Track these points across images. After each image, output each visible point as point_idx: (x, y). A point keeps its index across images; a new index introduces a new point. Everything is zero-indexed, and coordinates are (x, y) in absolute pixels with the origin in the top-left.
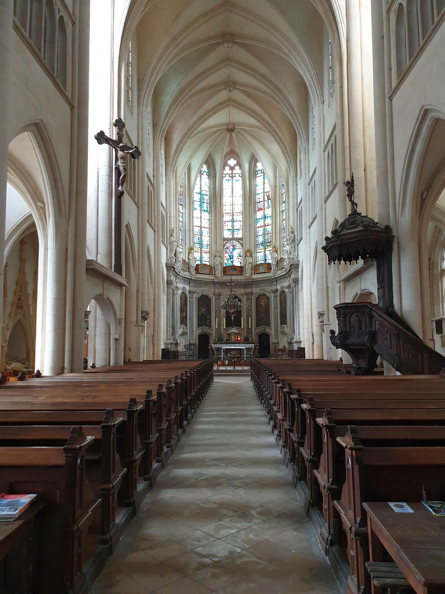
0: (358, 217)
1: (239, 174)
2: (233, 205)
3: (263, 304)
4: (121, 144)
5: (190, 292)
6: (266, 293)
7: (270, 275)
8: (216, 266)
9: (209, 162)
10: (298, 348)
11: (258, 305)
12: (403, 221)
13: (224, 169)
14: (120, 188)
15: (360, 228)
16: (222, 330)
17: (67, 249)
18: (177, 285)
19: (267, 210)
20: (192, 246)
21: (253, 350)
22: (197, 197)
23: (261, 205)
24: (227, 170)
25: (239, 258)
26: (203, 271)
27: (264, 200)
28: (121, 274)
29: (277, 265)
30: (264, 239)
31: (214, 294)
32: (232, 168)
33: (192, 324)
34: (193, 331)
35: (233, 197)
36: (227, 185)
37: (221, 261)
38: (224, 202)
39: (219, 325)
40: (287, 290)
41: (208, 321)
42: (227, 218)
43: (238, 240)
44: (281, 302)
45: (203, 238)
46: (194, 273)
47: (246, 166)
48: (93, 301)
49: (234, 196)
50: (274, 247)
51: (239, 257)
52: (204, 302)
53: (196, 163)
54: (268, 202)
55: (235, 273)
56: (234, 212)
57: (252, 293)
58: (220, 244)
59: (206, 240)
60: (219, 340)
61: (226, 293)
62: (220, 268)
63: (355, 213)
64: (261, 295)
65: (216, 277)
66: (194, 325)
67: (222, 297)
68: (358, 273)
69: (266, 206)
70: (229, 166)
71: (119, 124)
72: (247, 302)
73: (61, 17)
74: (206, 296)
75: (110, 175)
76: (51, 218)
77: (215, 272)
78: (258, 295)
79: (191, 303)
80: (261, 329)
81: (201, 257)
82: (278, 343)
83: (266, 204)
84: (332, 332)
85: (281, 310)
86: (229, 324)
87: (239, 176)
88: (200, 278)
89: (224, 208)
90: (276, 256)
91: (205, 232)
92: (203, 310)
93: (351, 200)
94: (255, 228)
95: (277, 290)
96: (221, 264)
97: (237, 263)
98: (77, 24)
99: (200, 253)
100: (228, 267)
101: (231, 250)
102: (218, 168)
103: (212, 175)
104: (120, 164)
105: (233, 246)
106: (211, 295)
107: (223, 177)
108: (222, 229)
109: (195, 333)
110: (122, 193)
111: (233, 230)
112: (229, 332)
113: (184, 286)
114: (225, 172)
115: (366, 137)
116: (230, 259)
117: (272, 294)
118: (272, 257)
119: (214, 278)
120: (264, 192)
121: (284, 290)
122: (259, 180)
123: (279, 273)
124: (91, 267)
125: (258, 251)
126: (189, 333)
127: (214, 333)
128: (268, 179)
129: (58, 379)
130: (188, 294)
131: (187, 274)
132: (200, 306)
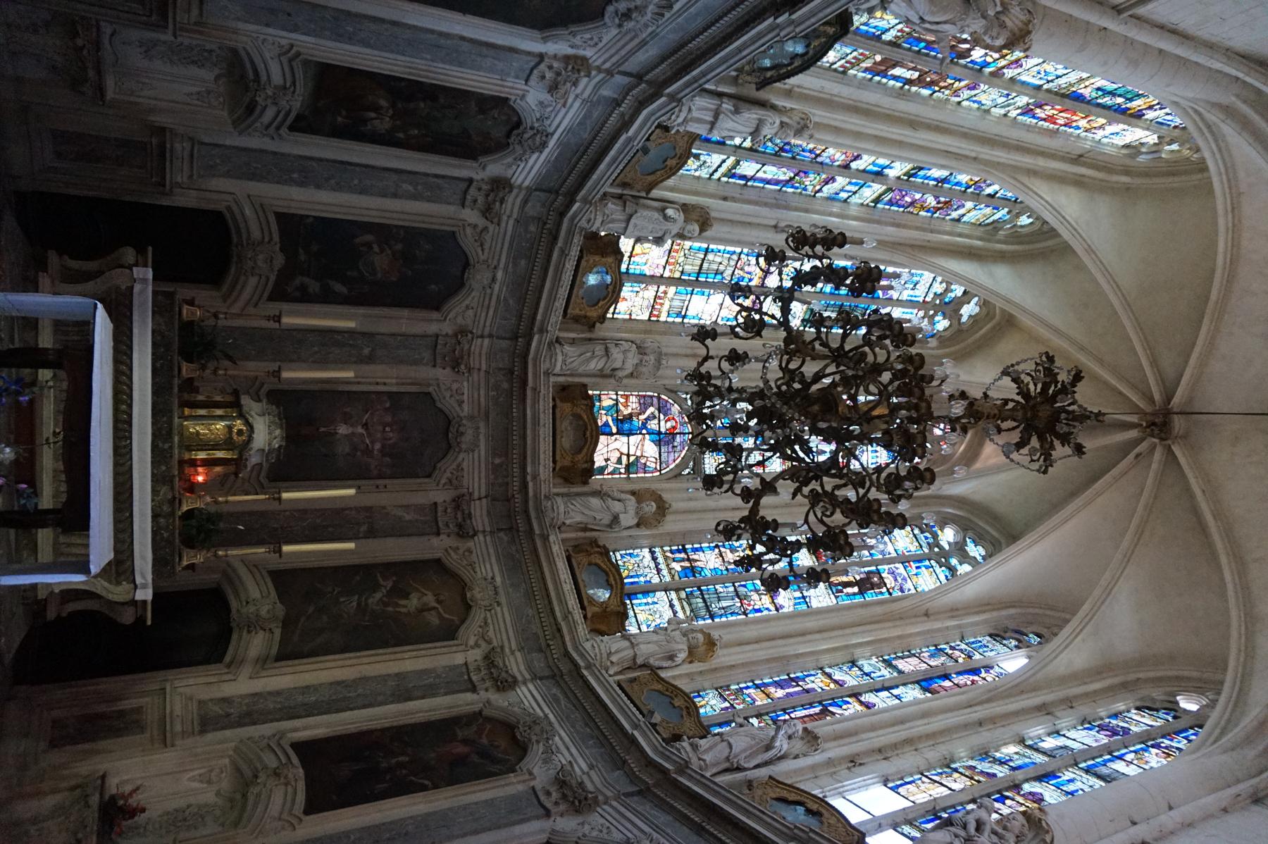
3: (413, 602)
5: (500, 185)
6: (477, 616)
11: (408, 573)
16: (254, 368)
25: (619, 461)
30: (714, 581)
31: (462, 332)
41: (314, 286)
51: (624, 458)
55: (566, 442)
60: (188, 327)
61: (464, 395)
62: (594, 365)
64: (462, 586)
67: (442, 374)
72: (420, 509)
74: (457, 285)
77: (573, 342)
78: (465, 574)
79: (430, 187)
81: (642, 279)
92: (381, 261)
95: (505, 684)
96: (609, 376)
99: (658, 272)
101: (653, 425)
105: (672, 434)
113: (552, 143)
116: (617, 421)
117: (475, 655)
120: (877, 563)
121: (537, 750)
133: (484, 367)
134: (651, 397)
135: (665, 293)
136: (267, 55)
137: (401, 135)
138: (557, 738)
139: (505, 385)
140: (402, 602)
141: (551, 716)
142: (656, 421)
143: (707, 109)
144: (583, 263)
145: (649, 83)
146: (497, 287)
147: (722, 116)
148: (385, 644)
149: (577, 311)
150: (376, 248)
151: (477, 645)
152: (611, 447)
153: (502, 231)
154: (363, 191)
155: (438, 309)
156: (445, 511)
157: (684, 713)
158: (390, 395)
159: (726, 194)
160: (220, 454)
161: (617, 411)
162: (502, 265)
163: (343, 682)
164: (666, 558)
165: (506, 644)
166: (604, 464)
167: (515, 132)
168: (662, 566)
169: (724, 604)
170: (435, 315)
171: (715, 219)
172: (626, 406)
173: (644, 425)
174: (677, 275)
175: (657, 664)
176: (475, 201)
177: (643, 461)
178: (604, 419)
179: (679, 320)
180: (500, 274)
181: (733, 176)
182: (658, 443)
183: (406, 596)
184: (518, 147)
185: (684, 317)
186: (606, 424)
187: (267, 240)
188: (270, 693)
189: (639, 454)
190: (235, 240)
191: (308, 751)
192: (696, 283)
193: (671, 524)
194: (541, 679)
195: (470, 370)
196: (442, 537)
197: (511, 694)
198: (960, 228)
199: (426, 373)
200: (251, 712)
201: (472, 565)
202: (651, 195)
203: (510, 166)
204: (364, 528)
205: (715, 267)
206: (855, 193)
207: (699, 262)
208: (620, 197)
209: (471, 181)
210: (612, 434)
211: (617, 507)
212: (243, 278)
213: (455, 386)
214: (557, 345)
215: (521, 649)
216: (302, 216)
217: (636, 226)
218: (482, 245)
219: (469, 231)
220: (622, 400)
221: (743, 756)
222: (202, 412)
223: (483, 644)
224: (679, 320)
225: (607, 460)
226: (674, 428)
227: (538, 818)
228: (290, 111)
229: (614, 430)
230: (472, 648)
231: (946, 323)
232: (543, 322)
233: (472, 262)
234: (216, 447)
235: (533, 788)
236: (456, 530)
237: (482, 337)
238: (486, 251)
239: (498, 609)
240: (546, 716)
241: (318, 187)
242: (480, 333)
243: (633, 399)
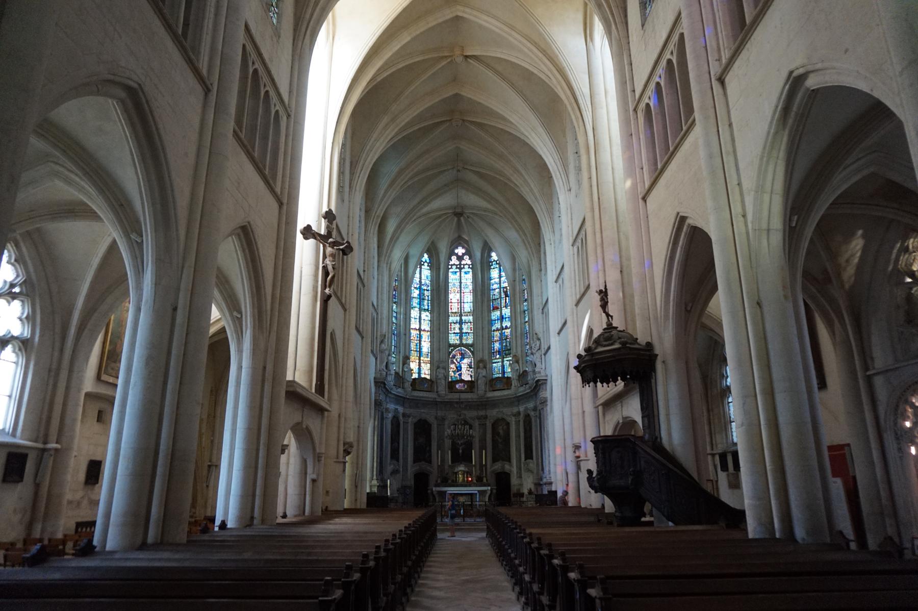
0: (614, 332)
3: (501, 432)
4: (331, 240)
6: (505, 417)
9: (432, 250)
11: (495, 432)
12: (665, 342)
14: (327, 291)
15: (617, 346)
16: (446, 467)
17: (265, 368)
21: (488, 495)
22: (415, 293)
23: (496, 304)
24: (454, 260)
27: (501, 298)
28: (323, 396)
31: (436, 418)
32: (460, 258)
33: (405, 459)
36: (453, 278)
39: (443, 461)
40: (532, 413)
43: (467, 346)
45: (423, 343)
47: (478, 255)
48: (290, 431)
50: (515, 356)
52: (423, 429)
53: (414, 252)
57: (486, 417)
58: (442, 353)
59: (426, 347)
60: (442, 482)
62: (443, 382)
63: (610, 327)
65: (439, 396)
67: (446, 423)
68: (617, 398)
69: (503, 304)
70: (457, 255)
71: (329, 216)
73: (277, 112)
75: (316, 275)
76: (249, 332)
79: (406, 430)
80: (498, 466)
81: (419, 369)
84: (590, 472)
85: (526, 438)
91: (426, 336)
93: (605, 312)
94: (490, 331)
95: (519, 413)
96: (446, 376)
97: (466, 377)
98: (292, 116)
103: (435, 266)
104: (328, 262)
106: (431, 420)
109: (409, 472)
110: (329, 297)
111: (461, 334)
114: (451, 263)
115: (621, 234)
117: (513, 419)
120: (500, 288)
122: (494, 273)
123: (522, 390)
124: (291, 389)
129: (248, 532)
130: (401, 418)
132: (416, 435)
193: (486, 358)
200: (519, 468)
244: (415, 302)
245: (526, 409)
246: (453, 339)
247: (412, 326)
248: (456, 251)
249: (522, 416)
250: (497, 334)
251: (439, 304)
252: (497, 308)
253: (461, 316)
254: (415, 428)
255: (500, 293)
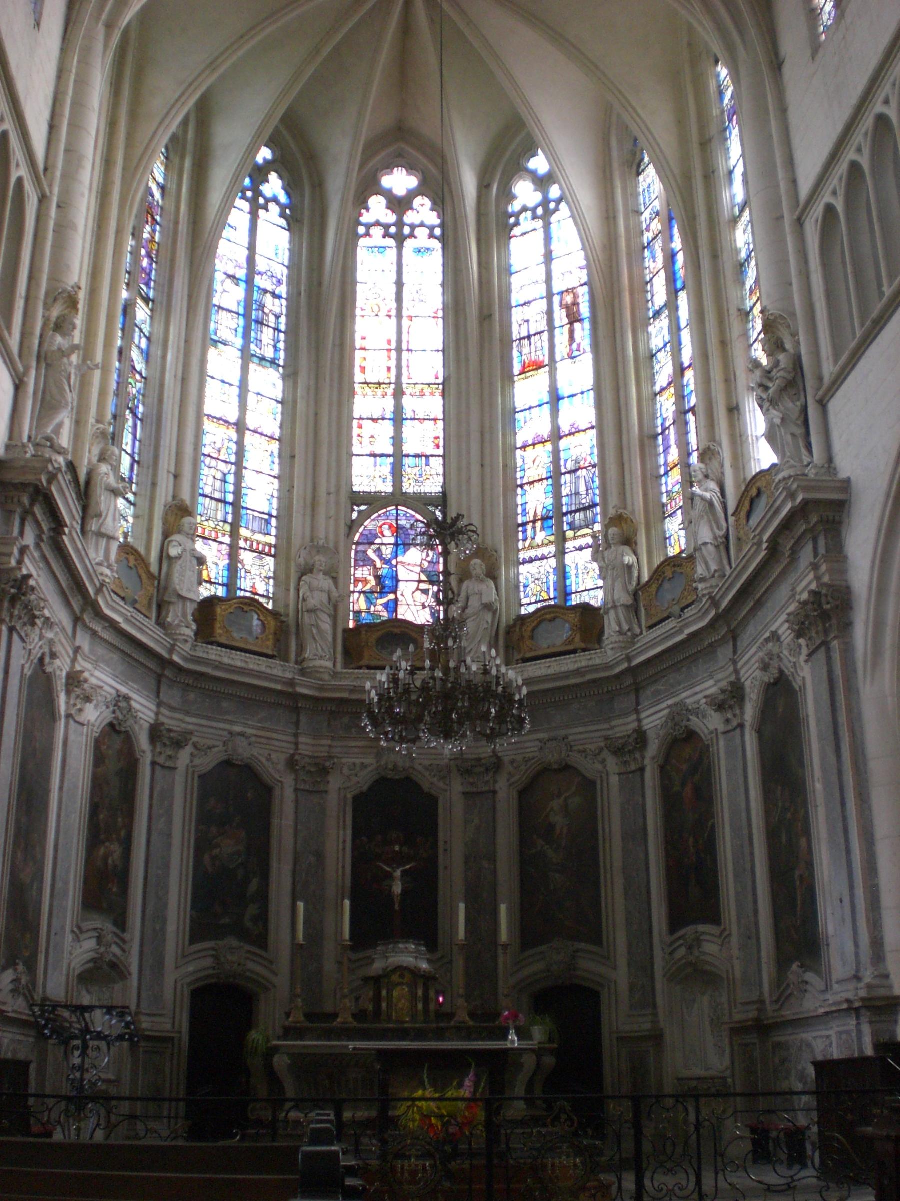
1: (432, 228)
2: (399, 350)
3: (558, 820)
5: (156, 732)
6: (576, 759)
7: (609, 654)
8: (307, 619)
10: (877, 1046)
13: (362, 203)
18: (78, 667)
19: (564, 368)
20: (186, 496)
22: (228, 295)
24: (377, 209)
25: (426, 592)
26: (237, 636)
29: (634, 608)
31: (292, 763)
32: (399, 205)
33: (156, 918)
34: (160, 963)
35: (399, 316)
36: (373, 265)
37: (335, 594)
38: (358, 337)
41: (253, 910)
42: (366, 404)
44: (671, 802)
45: (249, 478)
46: (189, 631)
47: (469, 182)
49: (405, 313)
51: (423, 586)
52: (235, 800)
54: (572, 333)
56: (405, 380)
59: (262, 494)
61: (357, 762)
62: (326, 625)
65: (303, 672)
66: (171, 927)
67: (335, 783)
70: (388, 195)
81: (233, 568)
82: (657, 1038)
83: (561, 337)
86: (376, 921)
87: (432, 236)
88: (219, 666)
89: (358, 362)
90: (629, 559)
91: (262, 457)
92: (229, 847)
95: (641, 738)
99: (225, 549)
100: (370, 626)
101: (387, 552)
102: (337, 183)
105: (397, 530)
107: (358, 237)
108: (343, 456)
109: (170, 977)
112: (378, 966)
113: (124, 690)
114: (366, 218)
116: (382, 593)
117: (612, 764)
118: (609, 572)
119: (289, 675)
121: (695, 722)
123: (653, 642)
125: (522, 556)
126: (134, 969)
127: (282, 980)
128: (577, 216)
130: (143, 741)
131: (148, 634)
133: (329, 742)
134: (357, 552)
135: (246, 540)
136: (79, 951)
137: (123, 833)
138: (688, 701)
139: (346, 719)
140: (558, 831)
141: (670, 702)
142: (383, 548)
143: (97, 545)
144: (223, 640)
145: (83, 610)
146: (249, 731)
147: (103, 530)
148: (595, 849)
149: (270, 643)
150: (216, 851)
151: (603, 761)
152: (411, 601)
153: (196, 728)
154: (167, 866)
155: (269, 790)
156: (472, 784)
157: (678, 570)
158: (355, 836)
159: (150, 483)
160: (420, 993)
161: (372, 593)
162: (228, 726)
163: (625, 889)
164: (531, 547)
165: (604, 733)
166: (428, 609)
167: (117, 727)
168: (539, 552)
169: (583, 489)
170: (277, 792)
171: (174, 497)
172: (365, 582)
173: (387, 562)
174: (228, 528)
175: (634, 584)
176: (170, 757)
177: (426, 565)
178: (380, 608)
179: (274, 522)
180: (237, 728)
181: (131, 478)
182: (407, 546)
183: (551, 827)
184: (128, 723)
185: (271, 516)
186: (386, 606)
187: (214, 953)
188: (629, 953)
189: (418, 569)
190: (213, 981)
191: (676, 922)
192: (237, 505)
194: (638, 704)
195: (330, 757)
196: (497, 787)
197: (651, 734)
198: (172, 187)
199: (333, 799)
200: (643, 966)
201: (526, 760)
202: (157, 574)
203: (141, 726)
204: (485, 864)
205: (218, 484)
206: (141, 330)
207: (214, 503)
208: (159, 607)
209: (154, 763)
210: (396, 601)
211: (474, 603)
212: (248, 974)
213: (346, 771)
214: (305, 664)
215: (609, 719)
216: (192, 921)
217: (189, 591)
218: (210, 748)
219: (197, 761)
220: (360, 587)
221: (717, 532)
222: (384, 1005)
223: (603, 755)
224: (274, 522)
225: (424, 606)
226: (391, 526)
227: (743, 735)
228: (115, 933)
229: (392, 597)
230: (605, 767)
231: (273, 176)
232: (285, 683)
233: (226, 757)
234: (414, 996)
235: (725, 733)
236: (491, 774)
237: (297, 744)
238: (218, 743)
239: (571, 738)
240: (669, 706)
241: (165, 905)
242: (293, 746)
243: (359, 574)
244: (226, 326)
245: (680, 713)
246: (369, 476)
247: (210, 406)
248: (387, 181)
249: (653, 748)
250: (544, 453)
251: (317, 347)
252: (539, 366)
253: (399, 393)
254: (203, 799)
255: (550, 313)
